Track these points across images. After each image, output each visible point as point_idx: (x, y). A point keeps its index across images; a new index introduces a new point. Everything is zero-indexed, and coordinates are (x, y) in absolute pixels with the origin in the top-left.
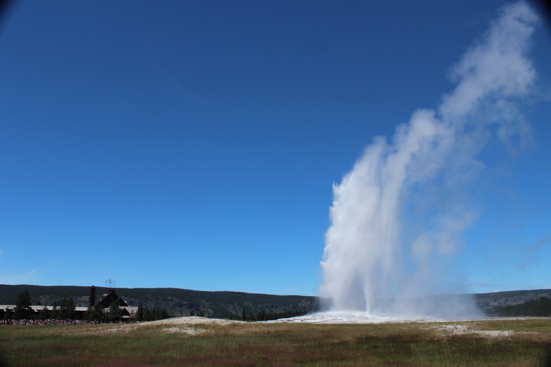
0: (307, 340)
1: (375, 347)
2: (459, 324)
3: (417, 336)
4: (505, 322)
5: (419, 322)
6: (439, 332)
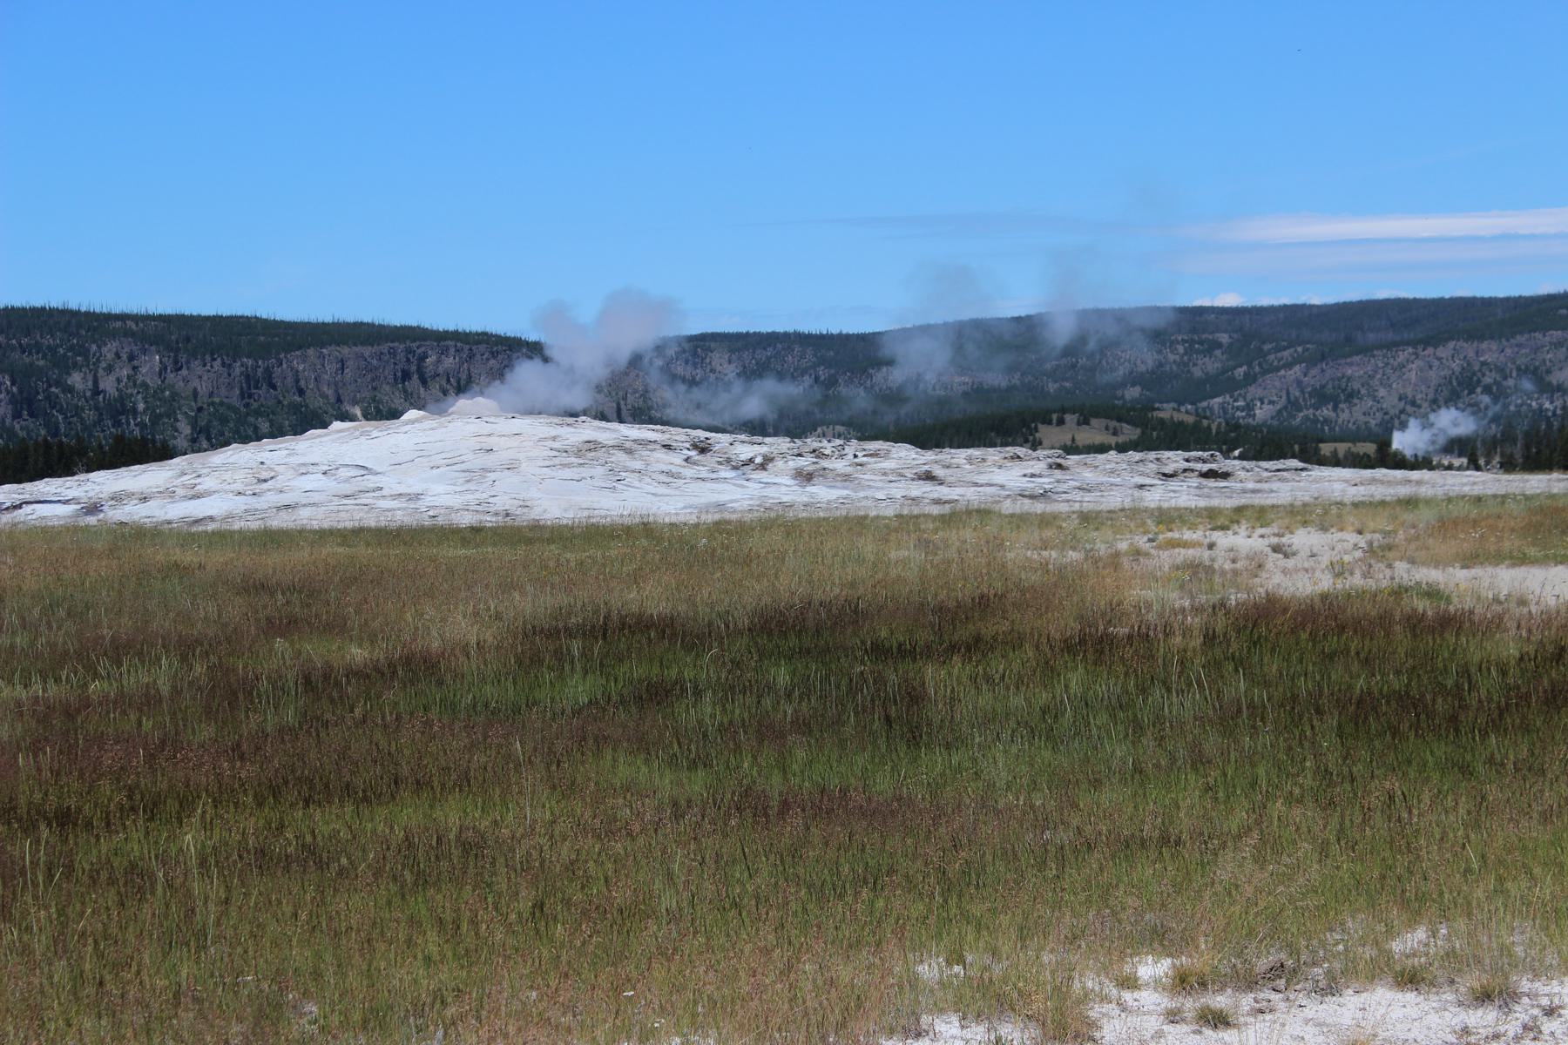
0: (118, 651)
1: (657, 694)
2: (1305, 524)
3: (983, 604)
5: (1008, 507)
6: (1151, 577)
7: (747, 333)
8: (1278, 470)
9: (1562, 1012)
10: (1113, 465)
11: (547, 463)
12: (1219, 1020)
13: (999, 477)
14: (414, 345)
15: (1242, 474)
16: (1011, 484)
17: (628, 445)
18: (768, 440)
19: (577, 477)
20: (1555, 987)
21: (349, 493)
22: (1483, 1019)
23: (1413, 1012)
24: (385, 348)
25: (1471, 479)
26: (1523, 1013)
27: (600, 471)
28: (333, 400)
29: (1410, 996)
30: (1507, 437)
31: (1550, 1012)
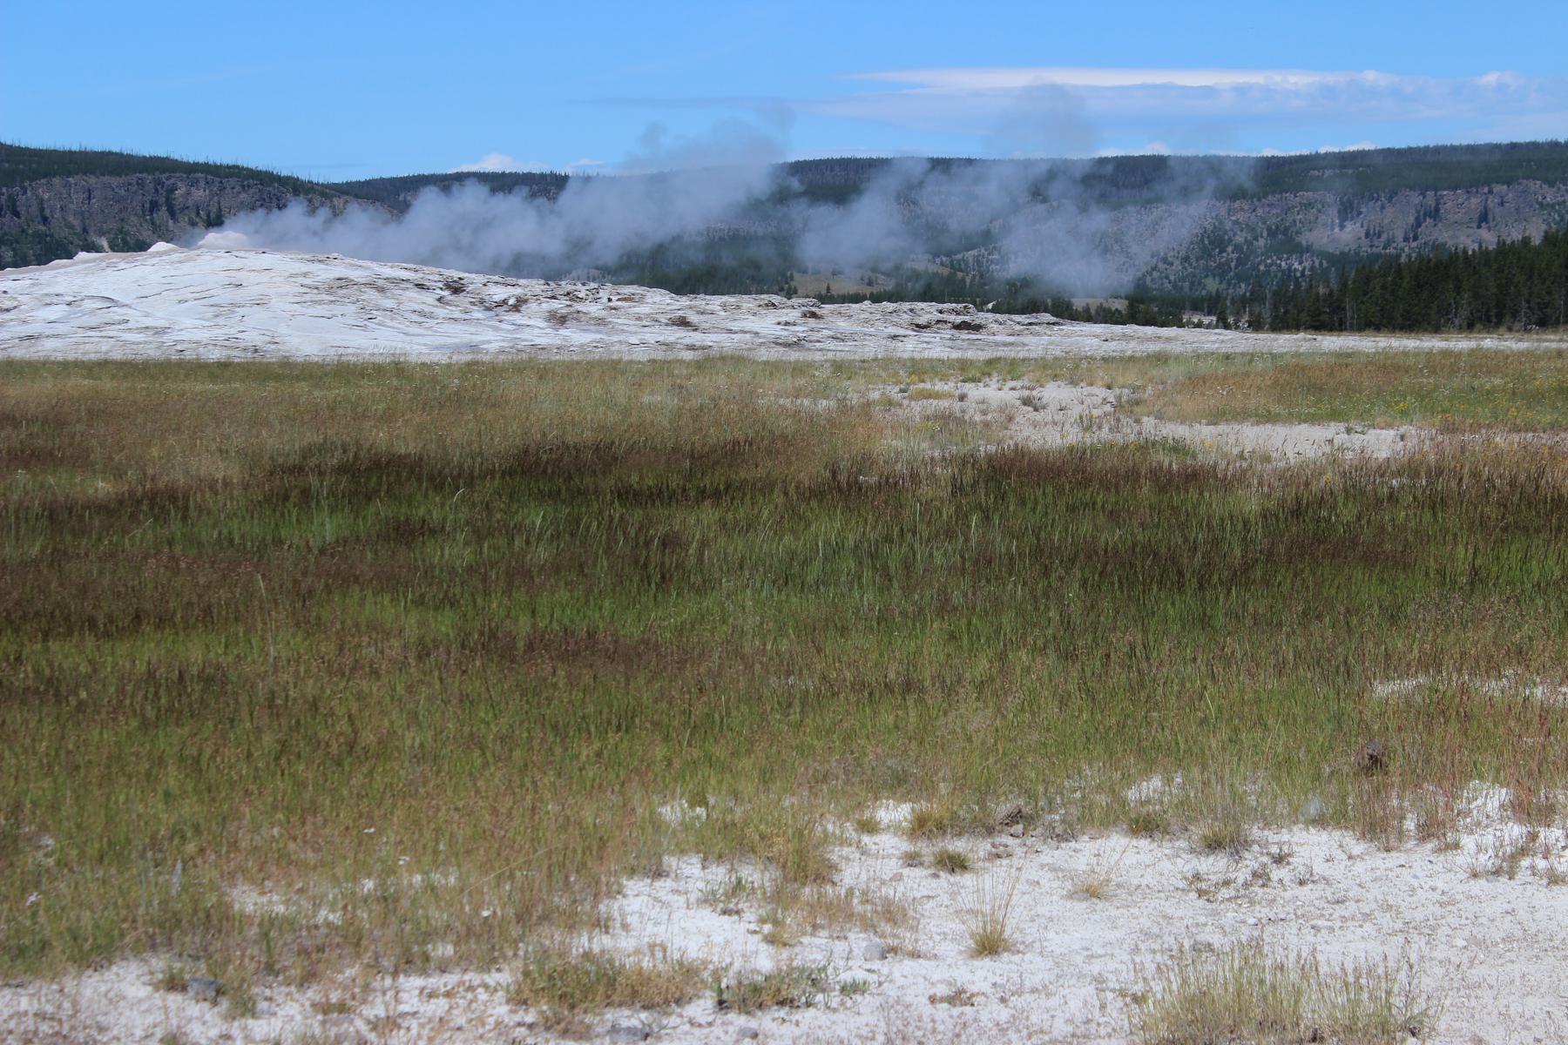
1: (405, 533)
2: (1055, 377)
3: (734, 452)
4: (1388, 366)
5: (764, 355)
7: (503, 173)
8: (1030, 324)
9: (1291, 860)
10: (867, 315)
11: (298, 299)
12: (955, 864)
13: (752, 323)
14: (164, 177)
15: (995, 327)
16: (766, 331)
17: (380, 283)
18: (522, 282)
19: (328, 314)
20: (1285, 836)
21: (93, 325)
22: (1214, 866)
23: (1145, 858)
24: (133, 178)
25: (1221, 337)
26: (1252, 860)
27: (352, 308)
28: (79, 230)
29: (1144, 843)
30: (1256, 297)
31: (1279, 860)
